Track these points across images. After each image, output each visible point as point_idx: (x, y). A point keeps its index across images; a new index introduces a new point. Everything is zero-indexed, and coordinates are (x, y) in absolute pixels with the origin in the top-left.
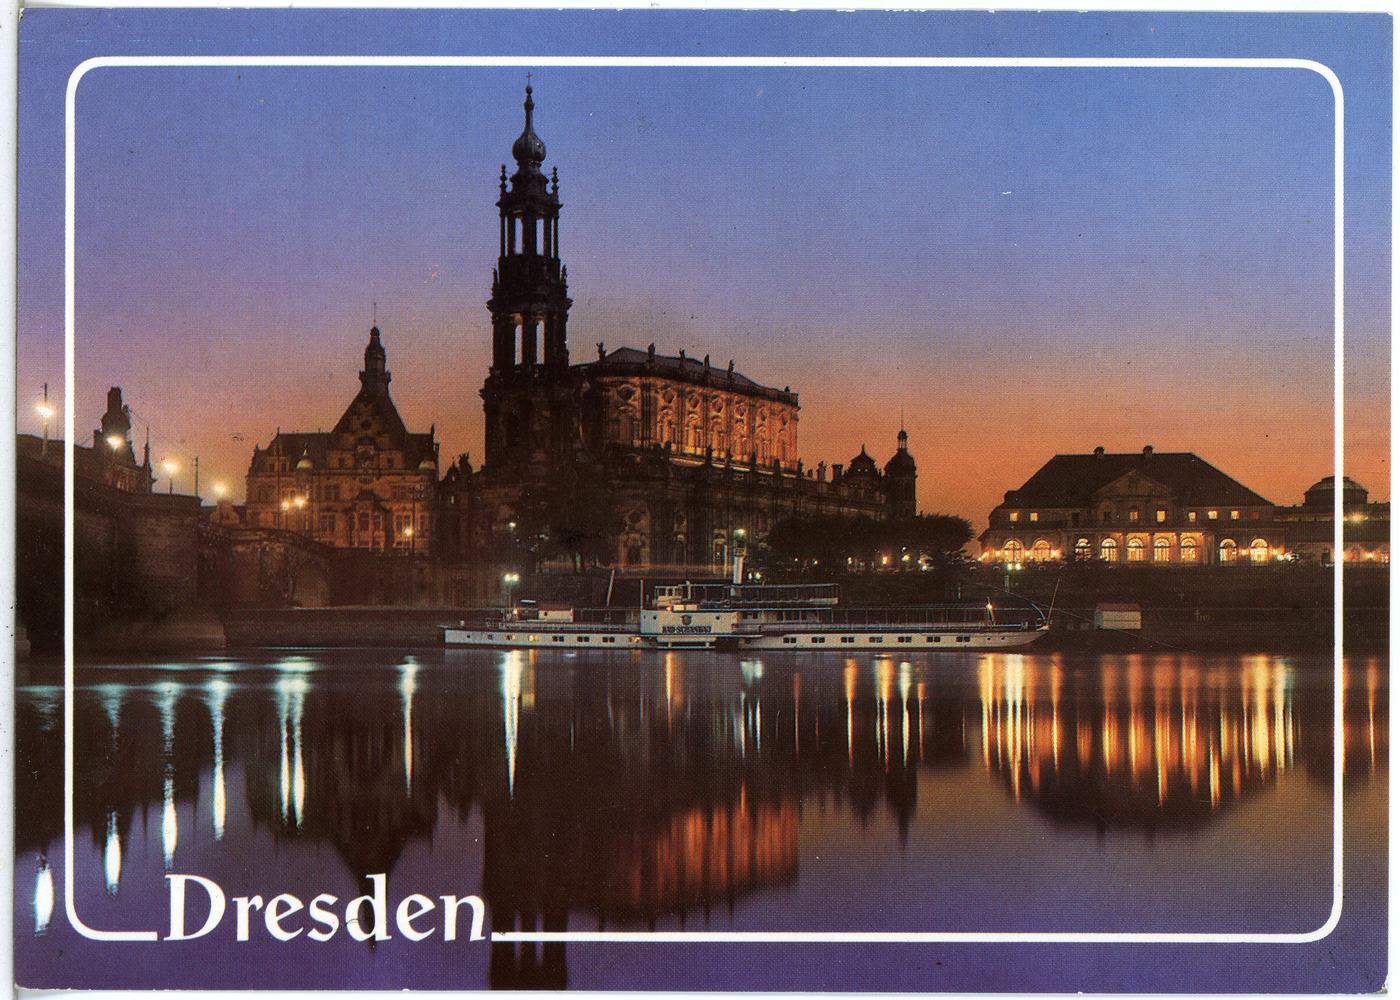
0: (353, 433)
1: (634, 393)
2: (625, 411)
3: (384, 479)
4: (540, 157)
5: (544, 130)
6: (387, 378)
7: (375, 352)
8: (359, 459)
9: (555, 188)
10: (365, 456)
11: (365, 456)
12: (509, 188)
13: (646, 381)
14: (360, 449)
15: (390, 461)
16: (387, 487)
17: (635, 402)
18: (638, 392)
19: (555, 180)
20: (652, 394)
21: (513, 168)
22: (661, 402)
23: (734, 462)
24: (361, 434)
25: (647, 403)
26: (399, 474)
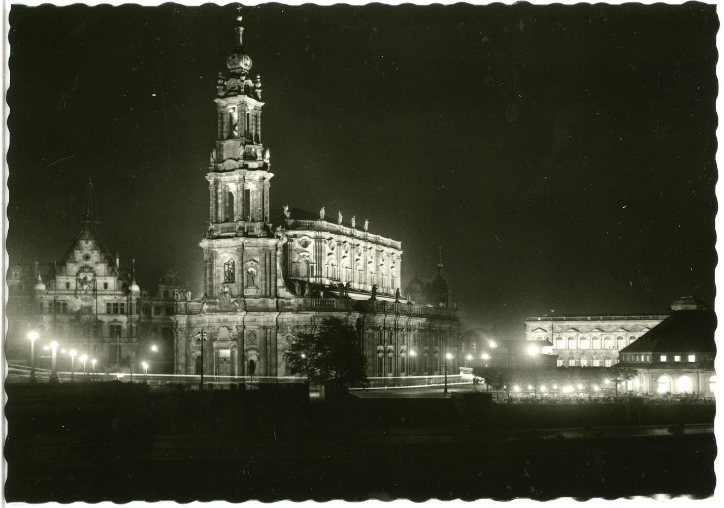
1: (310, 243)
2: (303, 256)
10: (84, 281)
11: (84, 281)
13: (319, 234)
14: (82, 276)
17: (311, 249)
18: (313, 241)
20: (323, 244)
22: (328, 250)
23: (379, 294)
25: (318, 250)
26: (112, 295)
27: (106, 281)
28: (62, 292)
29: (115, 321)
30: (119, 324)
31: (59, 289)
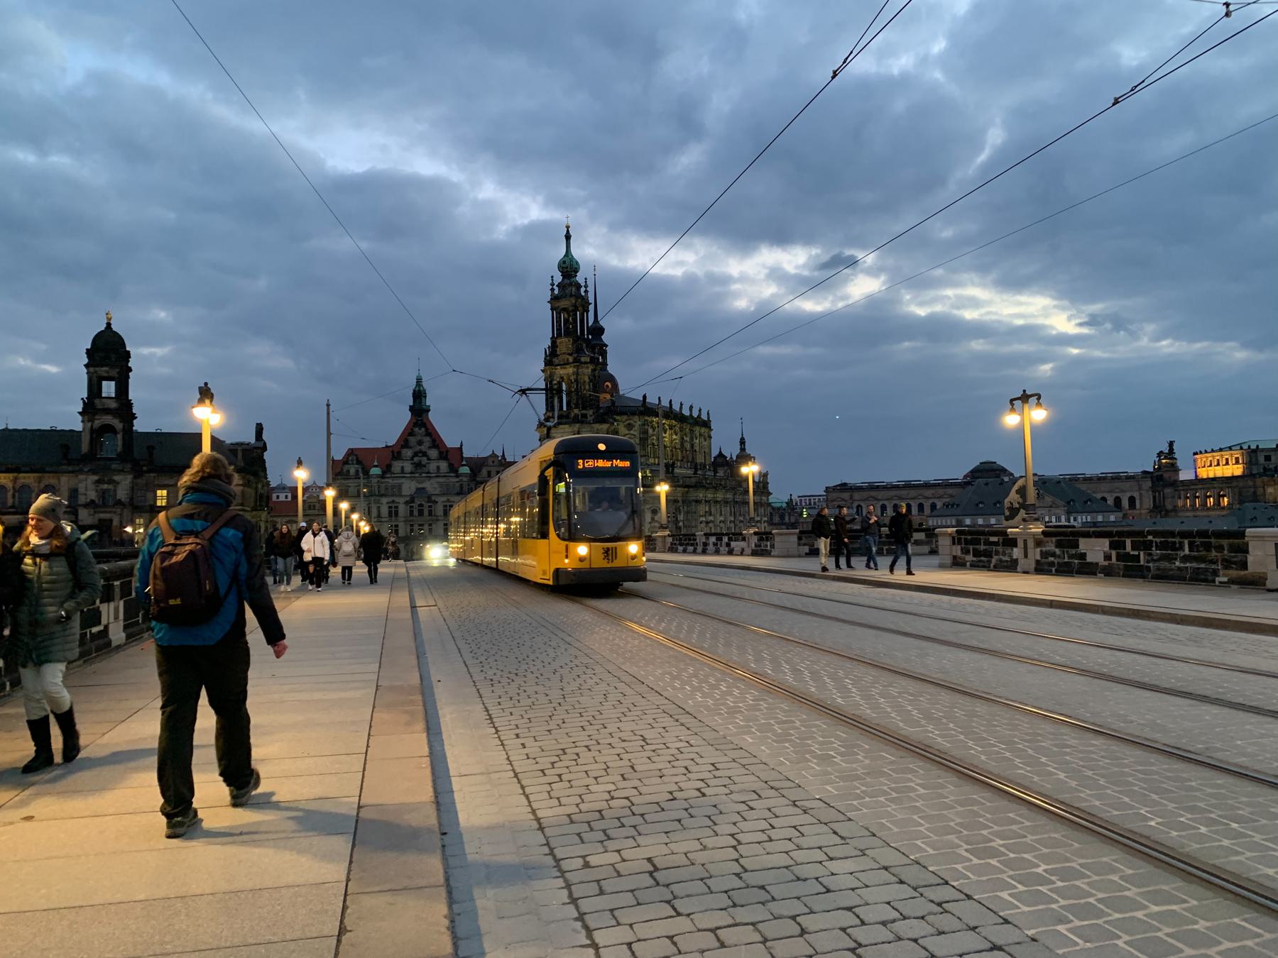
3: (433, 481)
4: (576, 271)
5: (575, 252)
7: (419, 395)
8: (418, 466)
9: (586, 292)
12: (556, 292)
15: (438, 468)
19: (586, 286)
21: (558, 278)
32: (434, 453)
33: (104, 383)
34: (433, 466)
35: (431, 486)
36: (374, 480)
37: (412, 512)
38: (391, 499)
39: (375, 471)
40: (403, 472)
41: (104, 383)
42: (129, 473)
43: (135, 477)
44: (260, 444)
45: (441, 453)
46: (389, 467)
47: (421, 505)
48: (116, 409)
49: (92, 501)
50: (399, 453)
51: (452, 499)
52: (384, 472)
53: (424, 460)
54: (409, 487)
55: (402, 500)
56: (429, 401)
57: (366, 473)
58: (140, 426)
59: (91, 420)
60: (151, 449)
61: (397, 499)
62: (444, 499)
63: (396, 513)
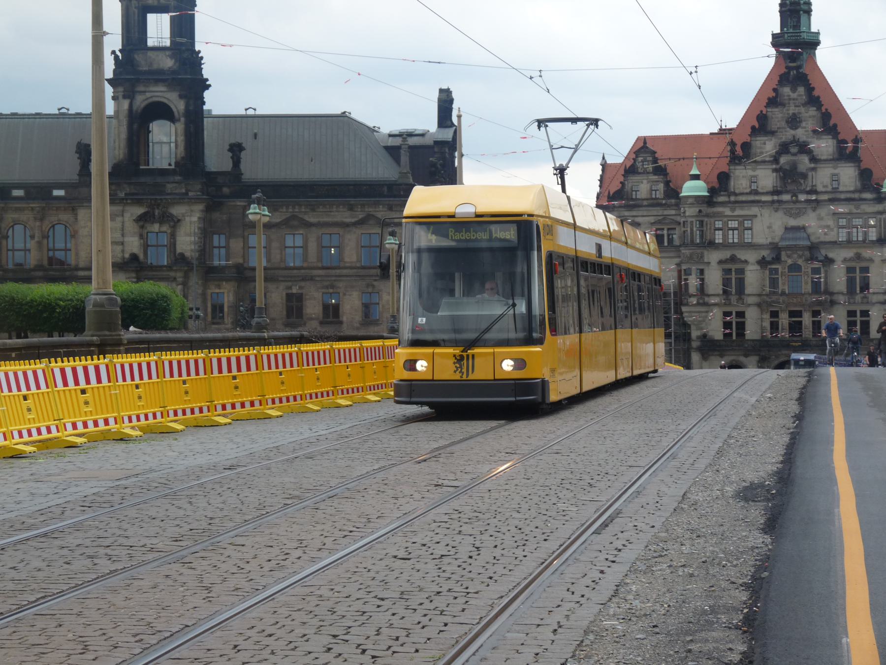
0: (773, 133)
3: (823, 211)
6: (813, 43)
8: (790, 178)
15: (835, 178)
16: (831, 223)
24: (788, 134)
27: (836, 171)
28: (743, 198)
29: (858, 257)
30: (864, 264)
31: (737, 191)
32: (824, 146)
33: (151, 18)
34: (822, 178)
35: (817, 224)
36: (691, 211)
37: (774, 283)
38: (726, 254)
39: (693, 188)
40: (756, 192)
41: (151, 18)
42: (197, 200)
43: (209, 209)
44: (447, 135)
45: (841, 142)
46: (724, 178)
47: (795, 268)
48: (173, 72)
49: (134, 257)
50: (746, 146)
51: (867, 253)
52: (712, 191)
53: (804, 162)
54: (767, 226)
55: (751, 257)
56: (818, 22)
57: (672, 193)
58: (218, 102)
59: (129, 95)
60: (236, 149)
61: (742, 255)
62: (849, 253)
63: (741, 283)
